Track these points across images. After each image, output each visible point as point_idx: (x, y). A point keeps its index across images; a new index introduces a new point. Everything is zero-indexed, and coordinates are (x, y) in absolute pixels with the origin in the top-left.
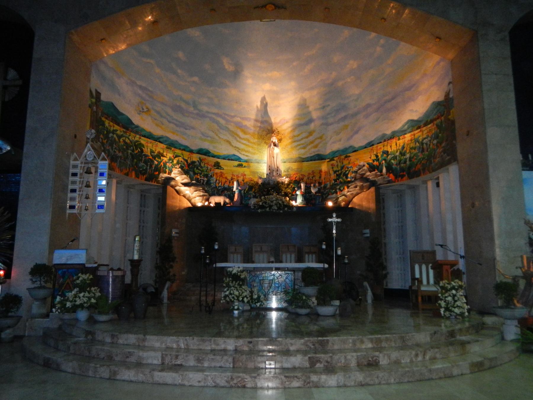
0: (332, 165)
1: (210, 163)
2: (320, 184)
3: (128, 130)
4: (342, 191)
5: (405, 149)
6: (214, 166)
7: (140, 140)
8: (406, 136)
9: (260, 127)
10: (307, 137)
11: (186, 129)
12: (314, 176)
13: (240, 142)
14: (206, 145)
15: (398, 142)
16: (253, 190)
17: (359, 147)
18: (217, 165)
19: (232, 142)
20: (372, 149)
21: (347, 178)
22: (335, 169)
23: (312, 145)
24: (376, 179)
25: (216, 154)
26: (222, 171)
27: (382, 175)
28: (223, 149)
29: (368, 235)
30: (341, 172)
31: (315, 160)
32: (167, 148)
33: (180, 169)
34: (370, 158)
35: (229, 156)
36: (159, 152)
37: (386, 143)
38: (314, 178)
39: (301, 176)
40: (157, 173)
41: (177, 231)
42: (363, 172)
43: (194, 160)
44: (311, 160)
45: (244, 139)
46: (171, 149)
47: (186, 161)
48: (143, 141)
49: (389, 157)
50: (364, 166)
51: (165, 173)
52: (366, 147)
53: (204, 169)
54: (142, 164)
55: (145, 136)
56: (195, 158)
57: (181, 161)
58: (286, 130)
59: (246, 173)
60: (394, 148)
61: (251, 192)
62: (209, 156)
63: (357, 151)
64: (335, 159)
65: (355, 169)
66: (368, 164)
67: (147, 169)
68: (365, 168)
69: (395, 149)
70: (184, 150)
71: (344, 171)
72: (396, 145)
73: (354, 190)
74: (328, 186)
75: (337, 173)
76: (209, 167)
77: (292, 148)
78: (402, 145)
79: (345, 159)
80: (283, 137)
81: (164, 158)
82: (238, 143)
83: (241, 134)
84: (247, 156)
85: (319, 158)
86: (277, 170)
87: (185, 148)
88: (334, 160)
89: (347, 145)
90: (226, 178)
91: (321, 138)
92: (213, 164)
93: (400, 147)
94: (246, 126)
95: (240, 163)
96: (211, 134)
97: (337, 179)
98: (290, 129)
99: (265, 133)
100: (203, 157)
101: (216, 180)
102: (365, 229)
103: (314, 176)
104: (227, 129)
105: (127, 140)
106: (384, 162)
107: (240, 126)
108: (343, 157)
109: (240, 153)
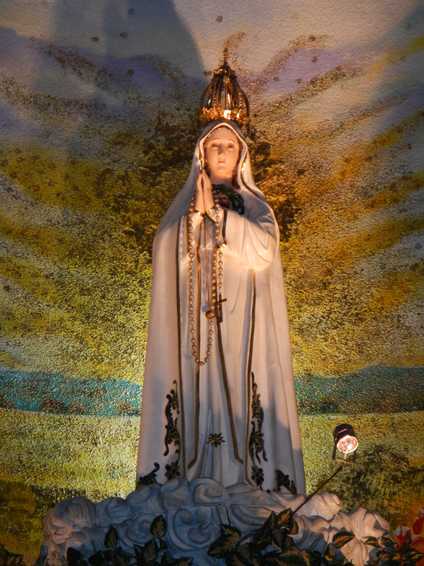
9: (94, 107)
77: (391, 279)
80: (301, 189)
86: (256, 440)
98: (367, 131)
99: (133, 156)
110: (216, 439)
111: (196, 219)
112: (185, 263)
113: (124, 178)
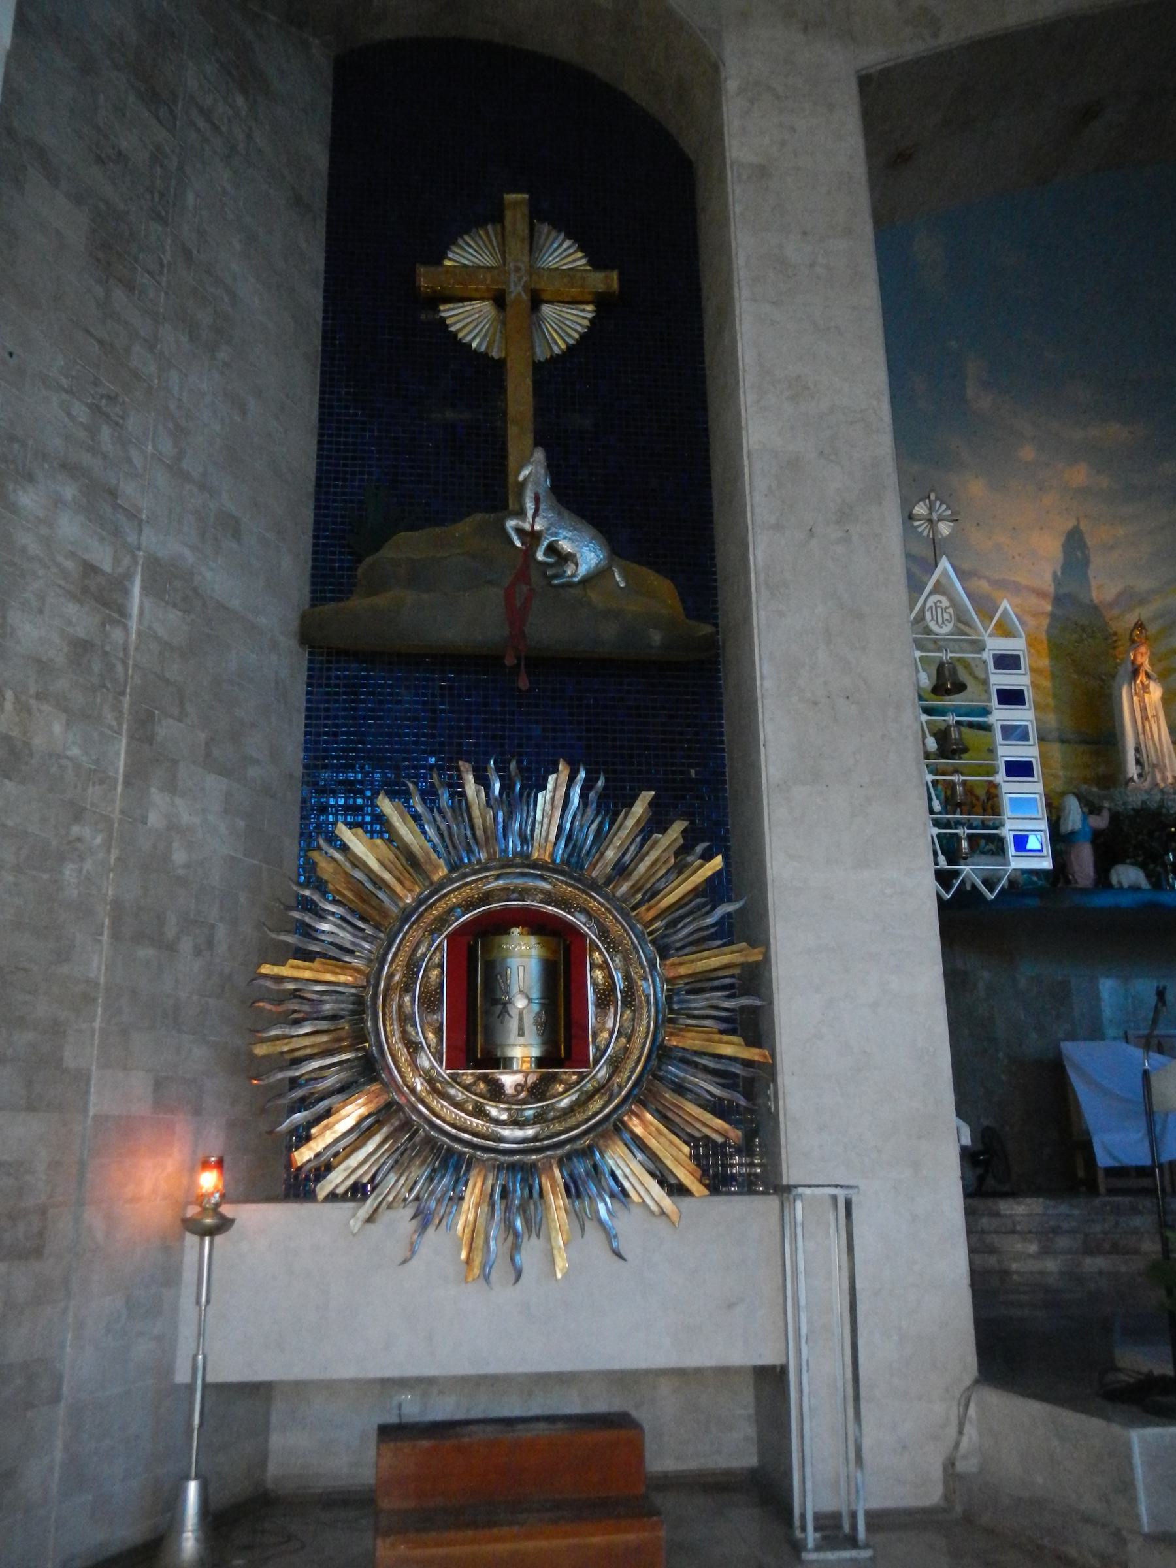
112: (1135, 699)
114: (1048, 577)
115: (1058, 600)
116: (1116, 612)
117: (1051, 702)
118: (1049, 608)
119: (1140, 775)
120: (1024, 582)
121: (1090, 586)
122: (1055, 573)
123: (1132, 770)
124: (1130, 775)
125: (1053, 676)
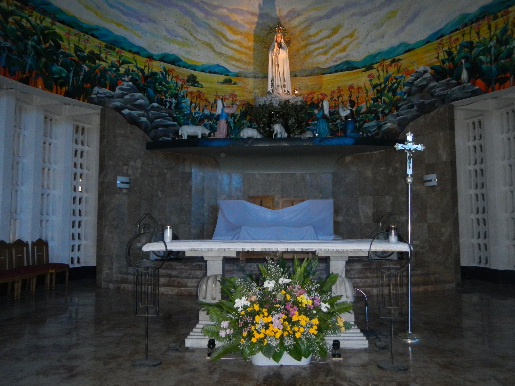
0: (369, 76)
1: (181, 77)
2: (352, 103)
3: (27, 5)
4: (386, 115)
5: (509, 32)
6: (188, 81)
7: (54, 27)
8: (510, 9)
10: (329, 37)
11: (141, 21)
12: (341, 95)
13: (227, 46)
14: (174, 49)
15: (493, 23)
16: (248, 117)
17: (418, 43)
18: (193, 80)
19: (215, 46)
20: (440, 44)
21: (394, 93)
22: (374, 82)
23: (338, 48)
24: (449, 91)
25: (190, 63)
26: (199, 89)
27: (459, 83)
28: (201, 57)
29: (434, 183)
30: (385, 86)
31: (341, 71)
32: (106, 46)
33: (131, 83)
34: (438, 58)
35: (209, 67)
36: (92, 52)
37: (467, 29)
38: (341, 98)
39: (320, 96)
40: (89, 85)
41: (125, 179)
42: (425, 83)
43: (155, 70)
44: (336, 71)
45: (232, 41)
46: (114, 50)
47: (142, 71)
48: (60, 29)
49: (475, 51)
50: (425, 72)
51: (105, 86)
52: (428, 42)
53: (171, 84)
54: (56, 68)
55: (63, 22)
56: (157, 67)
57: (133, 71)
58: (296, 27)
59: (237, 93)
60: (485, 34)
61: (244, 121)
62: (179, 66)
63: (413, 49)
64: (375, 66)
65: (409, 79)
66: (432, 68)
67: (68, 77)
68: (428, 75)
69: (487, 36)
70: (138, 53)
71: (389, 84)
72: (489, 28)
73: (407, 113)
74: (364, 110)
75: (379, 88)
76: (180, 83)
78: (501, 25)
79: (390, 65)
81: (101, 63)
82: (224, 48)
83: (229, 35)
84: (238, 67)
85: (349, 66)
87: (138, 52)
88: (372, 68)
89: (395, 42)
90: (206, 100)
91: (351, 36)
92: (186, 78)
93: (498, 32)
94: (236, 21)
95: (228, 77)
96: (181, 31)
97: (378, 97)
100: (169, 66)
101: (191, 103)
102: (427, 173)
103: (341, 95)
104: (210, 28)
105: (24, 22)
106: (463, 61)
107: (225, 21)
108: (388, 62)
109: (228, 63)
110: (278, 86)
111: (275, 50)
112: (273, 57)
113: (263, 37)
114: (257, 6)
115: (261, 16)
116: (287, 20)
117: (252, 61)
118: (256, 20)
119: (272, 91)
120: (245, 9)
121: (275, 8)
122: (259, 4)
123: (270, 88)
124: (268, 91)
125: (254, 50)
